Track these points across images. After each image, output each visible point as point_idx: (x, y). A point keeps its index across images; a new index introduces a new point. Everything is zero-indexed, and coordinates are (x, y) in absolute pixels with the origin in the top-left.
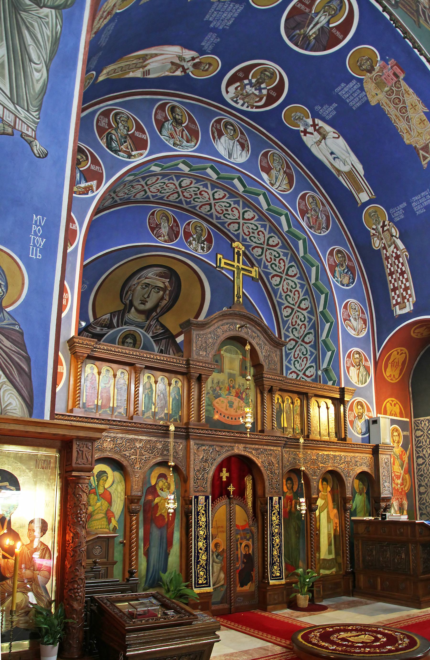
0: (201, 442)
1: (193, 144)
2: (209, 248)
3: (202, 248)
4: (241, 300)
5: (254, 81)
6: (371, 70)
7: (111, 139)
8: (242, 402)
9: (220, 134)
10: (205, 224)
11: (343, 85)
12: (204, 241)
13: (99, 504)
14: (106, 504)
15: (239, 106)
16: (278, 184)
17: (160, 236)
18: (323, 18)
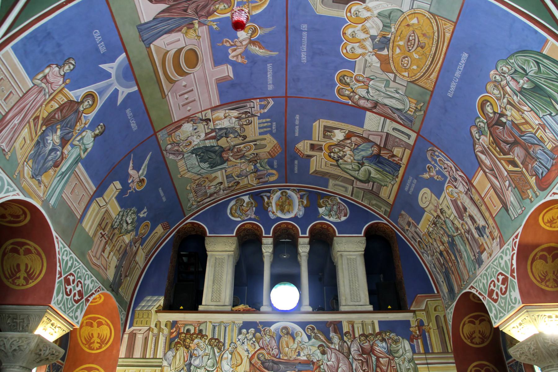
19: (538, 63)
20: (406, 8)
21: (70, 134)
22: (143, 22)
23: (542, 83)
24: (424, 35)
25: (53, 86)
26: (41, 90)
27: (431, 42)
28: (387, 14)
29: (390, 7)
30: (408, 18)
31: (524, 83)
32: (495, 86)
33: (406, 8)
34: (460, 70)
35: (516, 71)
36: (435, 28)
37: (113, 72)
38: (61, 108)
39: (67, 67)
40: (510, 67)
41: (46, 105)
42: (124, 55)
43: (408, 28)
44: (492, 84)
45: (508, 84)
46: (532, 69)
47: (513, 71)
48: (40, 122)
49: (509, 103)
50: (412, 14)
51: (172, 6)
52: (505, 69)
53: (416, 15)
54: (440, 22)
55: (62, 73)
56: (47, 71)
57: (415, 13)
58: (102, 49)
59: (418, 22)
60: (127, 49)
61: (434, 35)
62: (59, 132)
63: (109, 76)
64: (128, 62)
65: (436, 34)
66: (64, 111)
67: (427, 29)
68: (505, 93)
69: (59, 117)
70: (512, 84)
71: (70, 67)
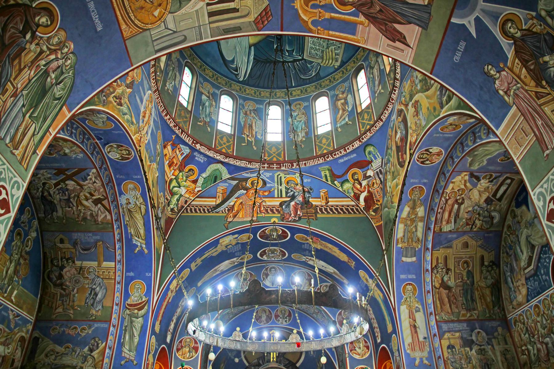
19: (59, 99)
20: (169, 18)
21: (547, 38)
22: (420, 29)
23: (46, 100)
24: (142, 8)
25: (510, 82)
26: (516, 95)
27: (132, 7)
28: (183, 3)
29: (183, 11)
30: (164, 11)
31: (52, 79)
32: (61, 42)
33: (169, 18)
34: (93, 11)
35: (62, 73)
36: (137, 22)
37: (472, 18)
38: (524, 63)
39: (492, 72)
40: (68, 68)
41: (526, 85)
42: (453, 20)
43: (159, 2)
44: (63, 40)
45: (57, 59)
46: (58, 91)
47: (64, 71)
48: (540, 90)
49: (42, 52)
50: (162, 17)
51: (391, 22)
52: (69, 62)
53: (158, 19)
54: (135, 30)
55: (498, 75)
56: (501, 92)
57: (160, 19)
58: (462, 45)
59: (153, 15)
60: (446, 22)
61: (134, 15)
62: (547, 58)
63: (477, 20)
64: (455, 11)
65: (133, 18)
66: (527, 57)
67: (142, 15)
68: (52, 51)
69: (532, 64)
70: (54, 65)
71: (491, 69)
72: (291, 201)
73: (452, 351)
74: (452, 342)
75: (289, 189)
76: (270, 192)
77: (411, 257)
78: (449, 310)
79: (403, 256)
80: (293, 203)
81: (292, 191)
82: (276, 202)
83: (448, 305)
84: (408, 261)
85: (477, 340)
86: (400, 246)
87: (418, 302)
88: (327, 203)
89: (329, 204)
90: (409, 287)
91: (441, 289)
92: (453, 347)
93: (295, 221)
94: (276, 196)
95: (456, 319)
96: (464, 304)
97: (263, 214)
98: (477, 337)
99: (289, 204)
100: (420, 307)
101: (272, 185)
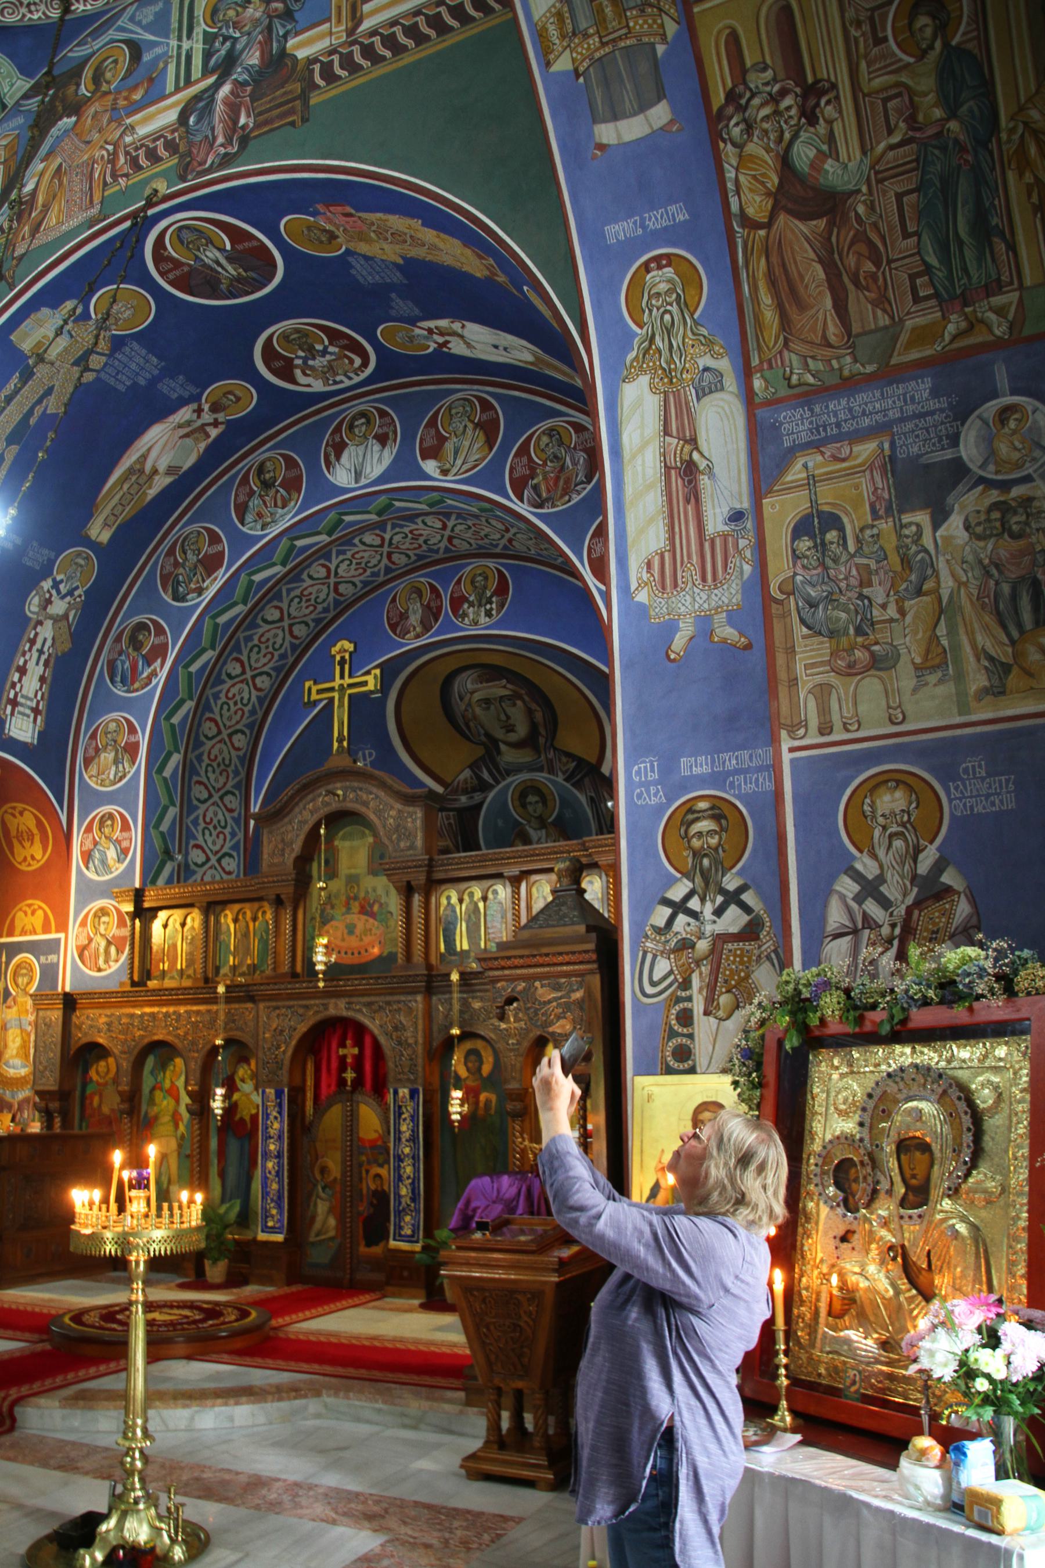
0: (274, 1004)
1: (293, 503)
2: (501, 605)
3: (489, 614)
4: (345, 744)
5: (301, 354)
6: (333, 237)
7: (178, 583)
8: (371, 920)
9: (339, 448)
10: (491, 563)
11: (353, 272)
12: (492, 596)
13: (165, 1102)
14: (172, 1102)
15: (348, 383)
16: (459, 462)
17: (409, 632)
18: (208, 253)
72: (217, 86)
73: (822, 547)
74: (827, 497)
75: (215, 36)
76: (151, 80)
77: (643, 107)
78: (833, 330)
79: (595, 121)
80: (226, 89)
81: (226, 39)
82: (162, 117)
83: (828, 303)
84: (628, 137)
85: (991, 455)
86: (563, 64)
87: (709, 343)
88: (350, 32)
89: (366, 25)
90: (661, 279)
91: (782, 218)
92: (833, 521)
93: (226, 160)
94: (170, 87)
95: (870, 369)
96: (928, 270)
97: (122, 181)
98: (989, 441)
99: (212, 100)
100: (724, 364)
101: (158, 50)
